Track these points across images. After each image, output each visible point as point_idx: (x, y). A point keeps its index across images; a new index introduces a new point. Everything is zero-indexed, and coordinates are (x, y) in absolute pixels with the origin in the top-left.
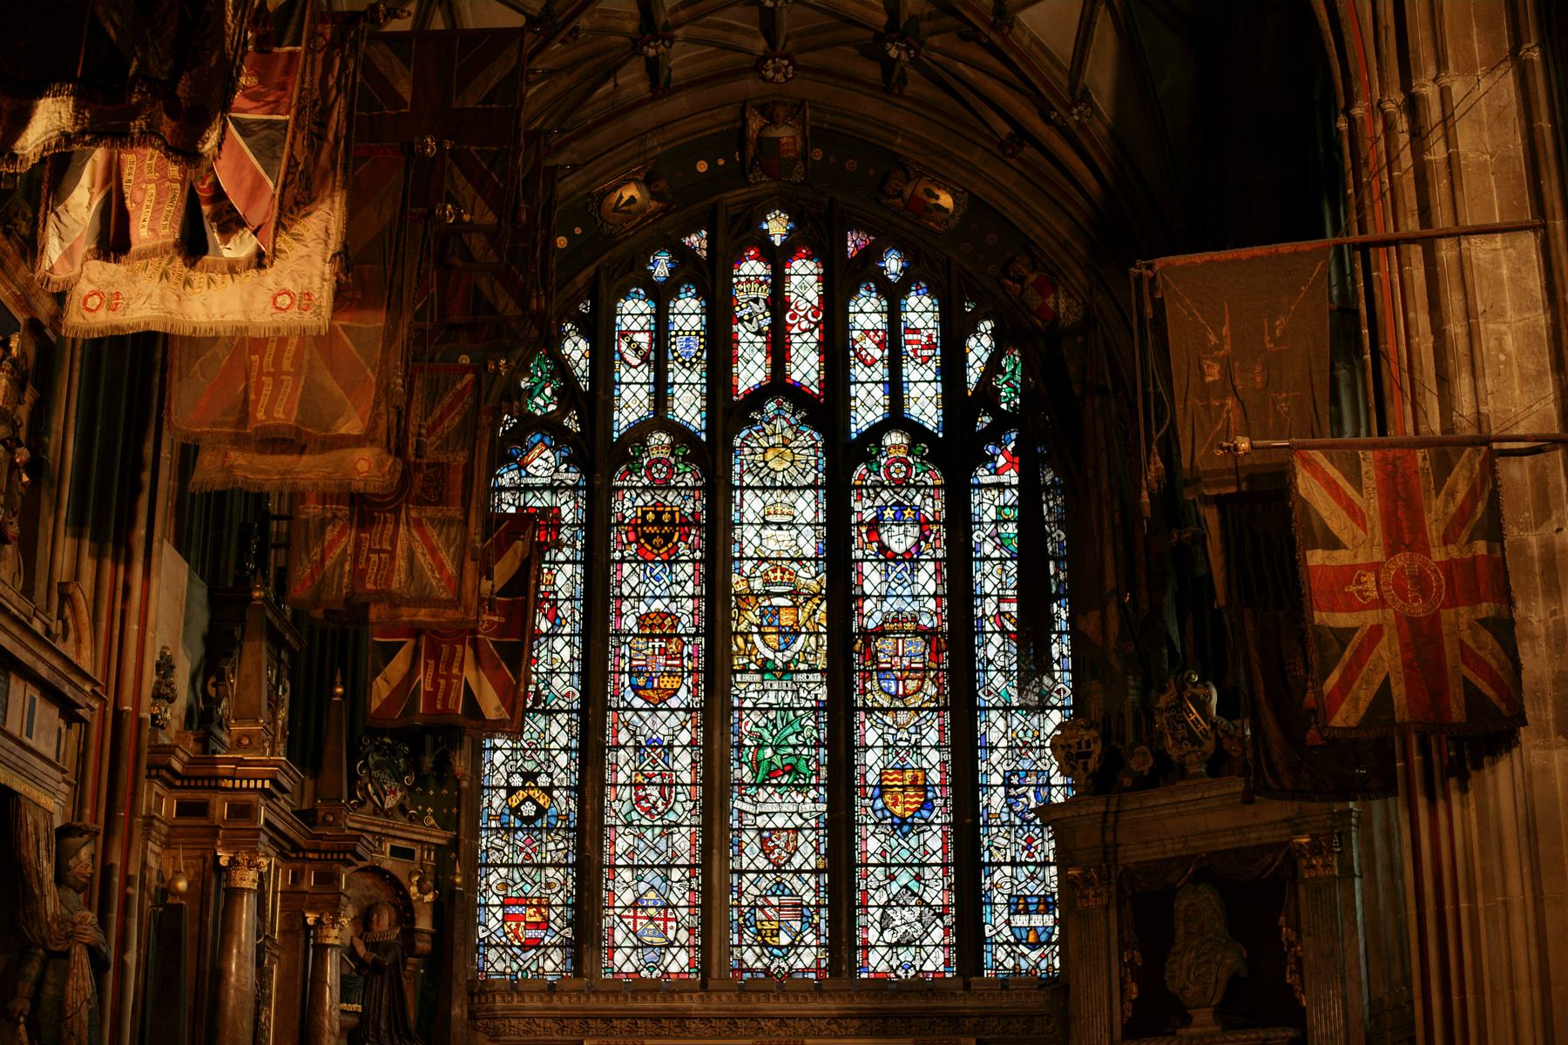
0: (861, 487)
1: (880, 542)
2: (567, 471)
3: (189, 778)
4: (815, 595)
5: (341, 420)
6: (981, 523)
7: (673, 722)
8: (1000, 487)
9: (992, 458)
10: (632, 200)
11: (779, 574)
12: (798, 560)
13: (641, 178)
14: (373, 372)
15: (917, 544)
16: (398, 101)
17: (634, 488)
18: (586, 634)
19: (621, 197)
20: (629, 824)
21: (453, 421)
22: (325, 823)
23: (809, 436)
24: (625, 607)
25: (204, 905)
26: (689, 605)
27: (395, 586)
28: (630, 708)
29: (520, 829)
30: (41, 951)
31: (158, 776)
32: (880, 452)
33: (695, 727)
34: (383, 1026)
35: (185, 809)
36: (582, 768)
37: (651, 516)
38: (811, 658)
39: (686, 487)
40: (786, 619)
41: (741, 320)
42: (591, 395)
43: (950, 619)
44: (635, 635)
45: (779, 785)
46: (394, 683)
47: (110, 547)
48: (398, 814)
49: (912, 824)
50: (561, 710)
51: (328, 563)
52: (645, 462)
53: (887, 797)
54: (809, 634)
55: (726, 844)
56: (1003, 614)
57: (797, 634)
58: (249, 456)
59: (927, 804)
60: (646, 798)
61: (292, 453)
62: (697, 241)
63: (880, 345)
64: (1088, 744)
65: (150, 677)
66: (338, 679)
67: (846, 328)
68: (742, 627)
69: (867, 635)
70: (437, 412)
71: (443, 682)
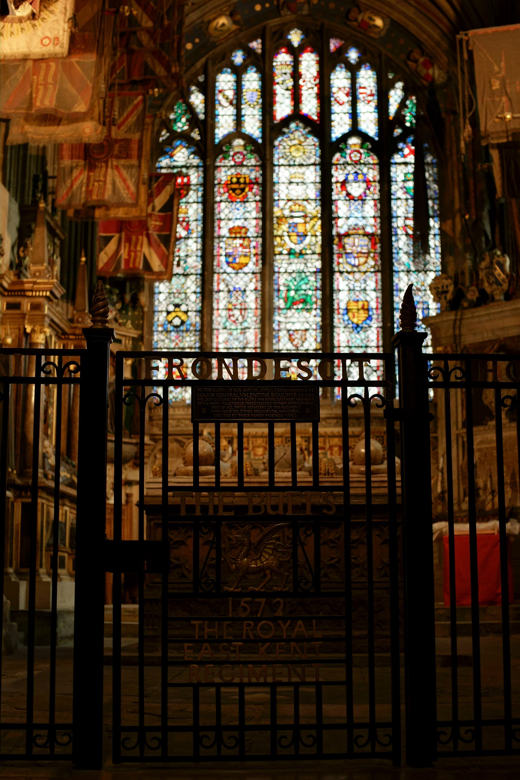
0: (337, 165)
1: (347, 191)
2: (193, 158)
4: (315, 217)
5: (76, 105)
6: (396, 181)
7: (246, 278)
8: (406, 164)
9: (401, 150)
10: (223, 25)
11: (297, 207)
12: (307, 200)
13: (228, 13)
14: (91, 81)
15: (365, 193)
17: (226, 166)
18: (204, 237)
19: (218, 24)
20: (225, 328)
21: (132, 119)
22: (78, 321)
23: (312, 140)
24: (222, 224)
26: (254, 222)
27: (106, 197)
28: (225, 272)
29: (173, 331)
32: (346, 147)
33: (257, 281)
36: (203, 301)
37: (234, 180)
38: (313, 248)
39: (252, 166)
40: (301, 229)
41: (278, 83)
42: (204, 121)
43: (381, 228)
44: (228, 238)
45: (298, 309)
49: (362, 328)
50: (192, 274)
51: (75, 187)
52: (232, 153)
53: (350, 314)
54: (312, 236)
55: (272, 337)
56: (406, 226)
57: (306, 236)
58: (34, 127)
59: (369, 318)
60: (233, 315)
61: (54, 125)
62: (256, 45)
63: (347, 95)
64: (447, 287)
66: (83, 254)
67: (329, 87)
68: (280, 233)
69: (340, 236)
70: (125, 114)
71: (133, 254)
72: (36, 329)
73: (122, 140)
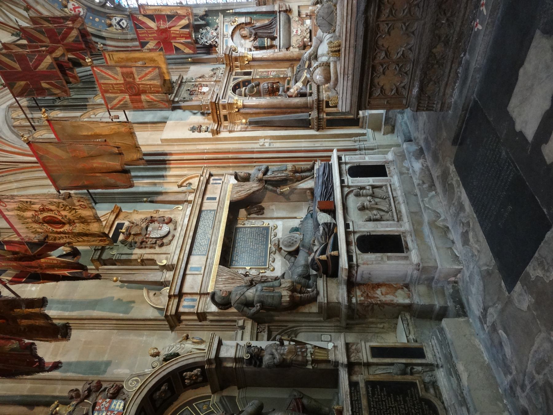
16: (27, 84)
21: (110, 73)
25: (247, 114)
27: (158, 84)
34: (270, 31)
35: (226, 118)
46: (185, 47)
47: (167, 166)
48: (217, 31)
51: (157, 100)
65: (196, 135)
70: (107, 76)
71: (182, 35)
72: (236, 107)
73: (123, 77)
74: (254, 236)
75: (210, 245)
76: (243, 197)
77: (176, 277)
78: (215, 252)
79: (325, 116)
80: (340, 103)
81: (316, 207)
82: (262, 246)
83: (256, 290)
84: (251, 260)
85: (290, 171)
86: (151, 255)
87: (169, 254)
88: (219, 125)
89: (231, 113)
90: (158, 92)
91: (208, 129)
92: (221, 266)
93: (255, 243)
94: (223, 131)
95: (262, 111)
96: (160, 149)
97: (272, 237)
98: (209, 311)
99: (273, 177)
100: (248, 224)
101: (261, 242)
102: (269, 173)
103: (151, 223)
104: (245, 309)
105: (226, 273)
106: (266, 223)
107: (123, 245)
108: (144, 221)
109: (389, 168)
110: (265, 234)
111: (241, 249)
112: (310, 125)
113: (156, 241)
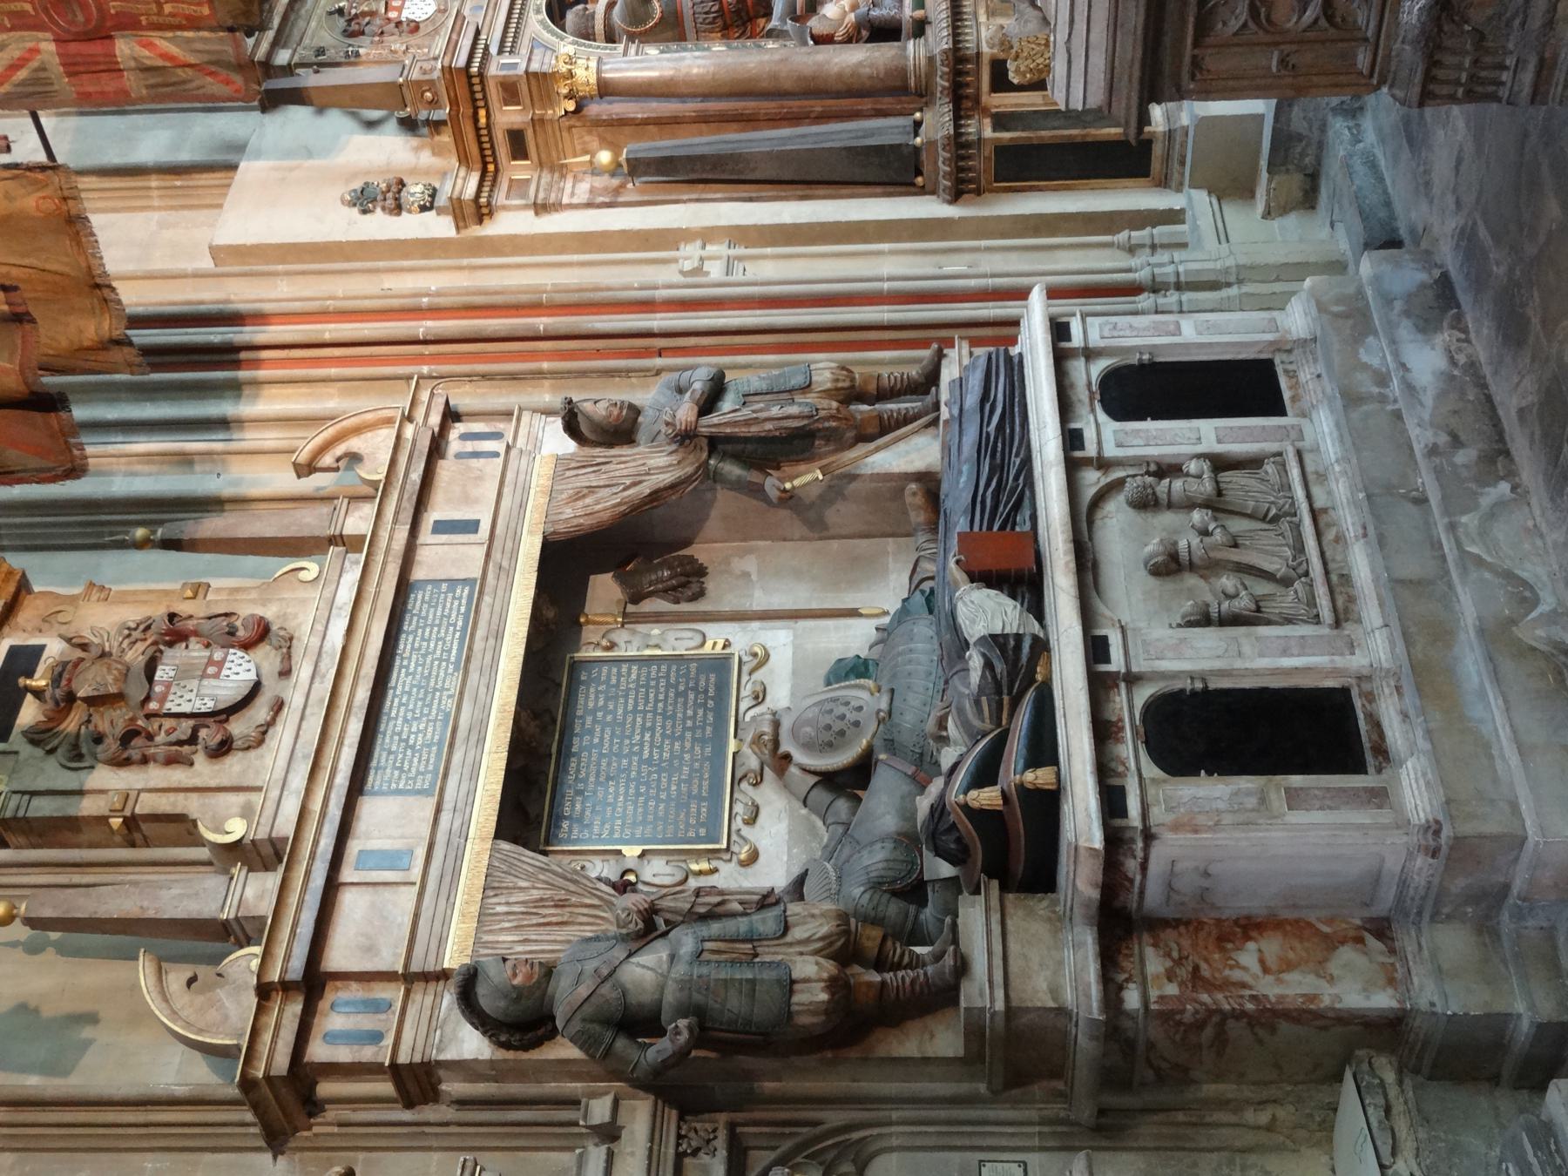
3: (483, 157)
25: (622, 122)
30: (712, 462)
31: (489, 204)
35: (519, 148)
47: (243, 374)
51: (192, 60)
65: (379, 226)
72: (565, 91)
74: (657, 701)
75: (452, 745)
76: (606, 516)
77: (293, 900)
78: (474, 776)
79: (988, 133)
80: (1059, 67)
81: (952, 564)
82: (697, 749)
83: (673, 958)
84: (645, 813)
85: (827, 393)
86: (172, 797)
87: (259, 789)
88: (489, 175)
89: (542, 121)
90: (193, 23)
91: (433, 195)
92: (505, 846)
93: (663, 736)
94: (505, 208)
95: (690, 107)
96: (207, 296)
97: (743, 706)
98: (449, 1055)
99: (748, 422)
100: (630, 644)
101: (693, 729)
102: (727, 404)
103: (170, 644)
104: (621, 1044)
105: (529, 876)
106: (716, 636)
107: (39, 752)
108: (136, 634)
109: (1292, 375)
110: (711, 693)
111: (599, 764)
112: (919, 173)
113: (195, 731)
